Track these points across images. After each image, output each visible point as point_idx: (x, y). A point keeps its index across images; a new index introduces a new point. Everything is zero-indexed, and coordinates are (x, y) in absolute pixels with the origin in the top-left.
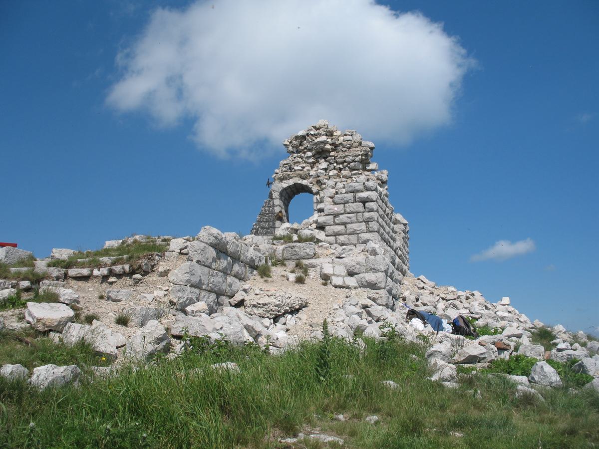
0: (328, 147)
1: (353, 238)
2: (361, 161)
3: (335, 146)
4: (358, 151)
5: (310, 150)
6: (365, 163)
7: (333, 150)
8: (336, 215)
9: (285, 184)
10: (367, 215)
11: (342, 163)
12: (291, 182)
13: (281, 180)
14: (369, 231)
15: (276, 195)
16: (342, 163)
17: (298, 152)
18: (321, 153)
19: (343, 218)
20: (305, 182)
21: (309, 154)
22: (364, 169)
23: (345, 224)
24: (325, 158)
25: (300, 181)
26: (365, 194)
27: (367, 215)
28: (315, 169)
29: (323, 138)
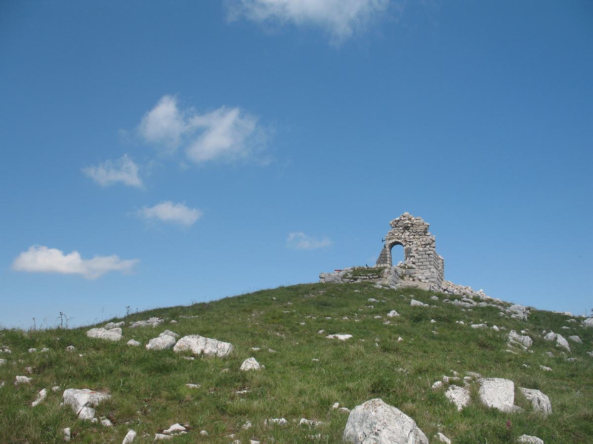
0: (409, 225)
1: (425, 267)
2: (424, 232)
3: (412, 224)
4: (423, 227)
5: (401, 226)
6: (425, 232)
7: (411, 226)
8: (419, 259)
9: (391, 242)
10: (430, 259)
11: (415, 232)
12: (394, 241)
13: (389, 239)
14: (430, 265)
15: (387, 246)
16: (415, 232)
17: (396, 227)
18: (406, 228)
19: (421, 260)
20: (399, 241)
21: (401, 228)
22: (425, 235)
23: (422, 262)
24: (408, 230)
25: (397, 240)
26: (429, 252)
27: (430, 259)
28: (404, 235)
29: (407, 222)
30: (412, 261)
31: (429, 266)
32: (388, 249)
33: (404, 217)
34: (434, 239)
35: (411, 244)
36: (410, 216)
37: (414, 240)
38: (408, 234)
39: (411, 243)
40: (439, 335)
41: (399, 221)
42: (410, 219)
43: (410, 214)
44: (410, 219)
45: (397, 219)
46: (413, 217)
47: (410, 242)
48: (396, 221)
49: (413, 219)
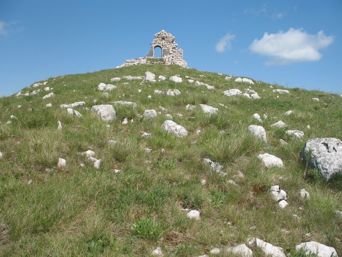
0: (165, 37)
1: (179, 60)
2: (172, 41)
3: (166, 37)
4: (172, 39)
5: (161, 37)
6: (173, 41)
7: (166, 38)
8: (176, 55)
9: (155, 45)
10: (181, 56)
11: (168, 41)
12: (156, 45)
13: (154, 44)
14: (181, 58)
15: (153, 47)
16: (168, 41)
17: (158, 37)
18: (163, 39)
19: (177, 56)
20: (159, 45)
21: (161, 38)
22: (172, 43)
23: (177, 57)
24: (164, 40)
25: (158, 45)
26: (181, 52)
27: (181, 56)
28: (162, 42)
29: (164, 35)
30: (172, 56)
31: (181, 59)
32: (153, 49)
33: (162, 32)
34: (177, 45)
35: (165, 47)
36: (165, 32)
37: (167, 45)
38: (164, 41)
39: (166, 47)
40: (179, 96)
41: (159, 34)
42: (165, 34)
43: (165, 31)
44: (165, 34)
45: (159, 33)
46: (167, 33)
47: (165, 46)
48: (158, 34)
49: (167, 34)
